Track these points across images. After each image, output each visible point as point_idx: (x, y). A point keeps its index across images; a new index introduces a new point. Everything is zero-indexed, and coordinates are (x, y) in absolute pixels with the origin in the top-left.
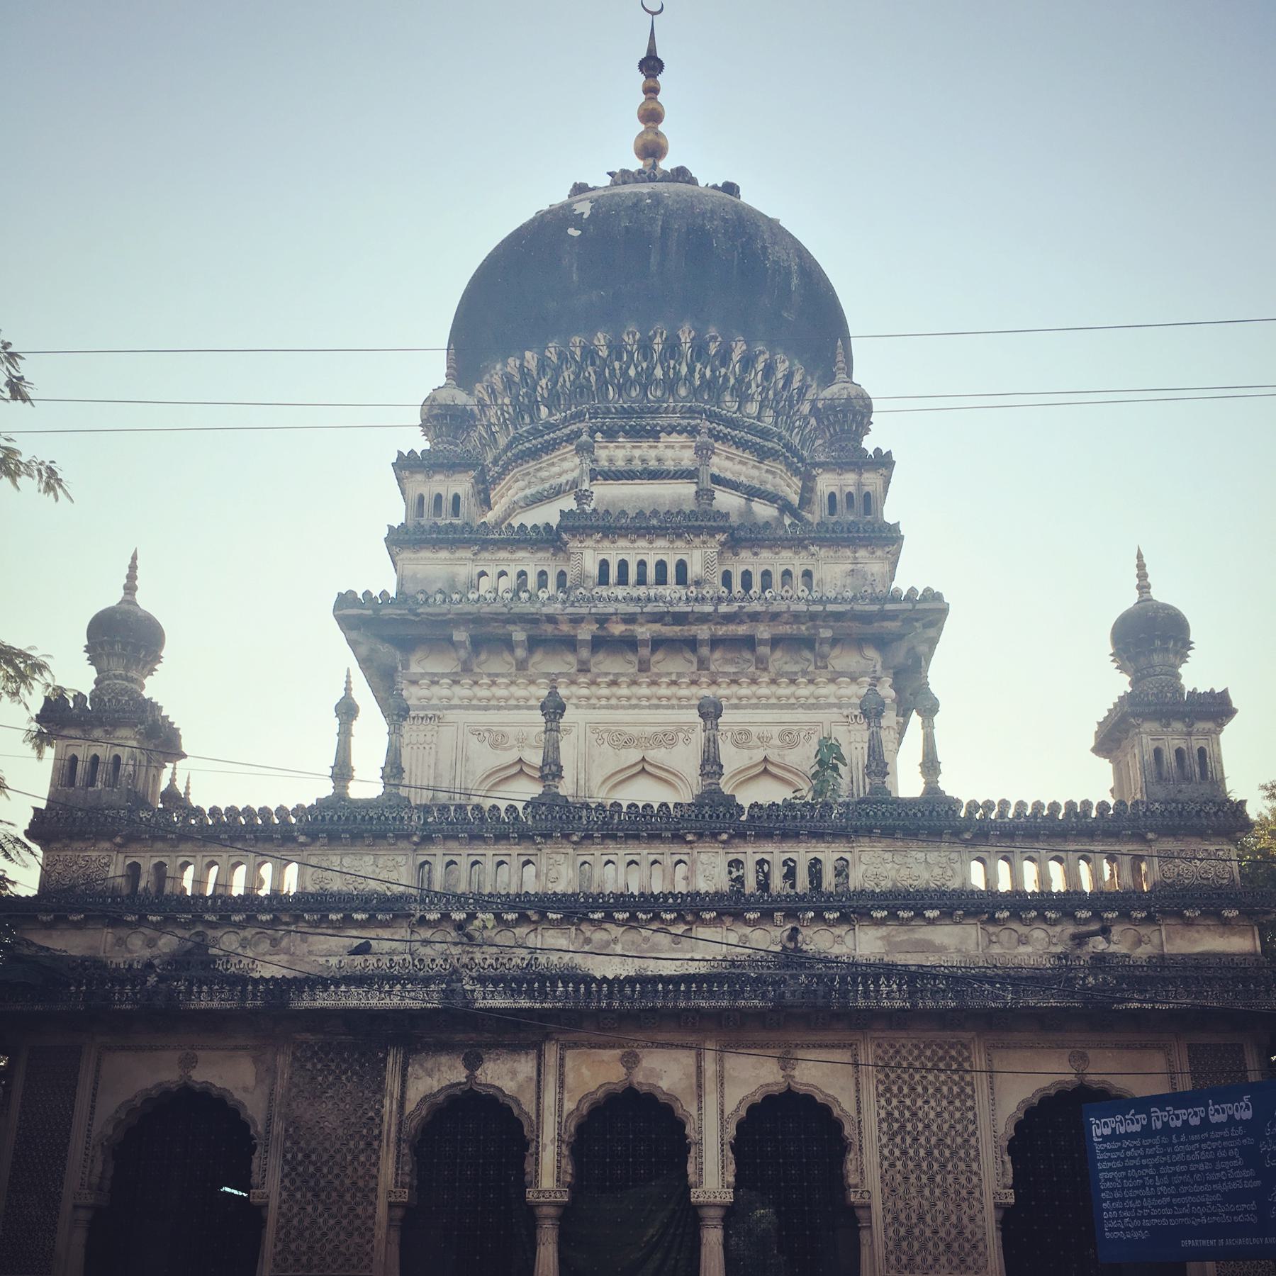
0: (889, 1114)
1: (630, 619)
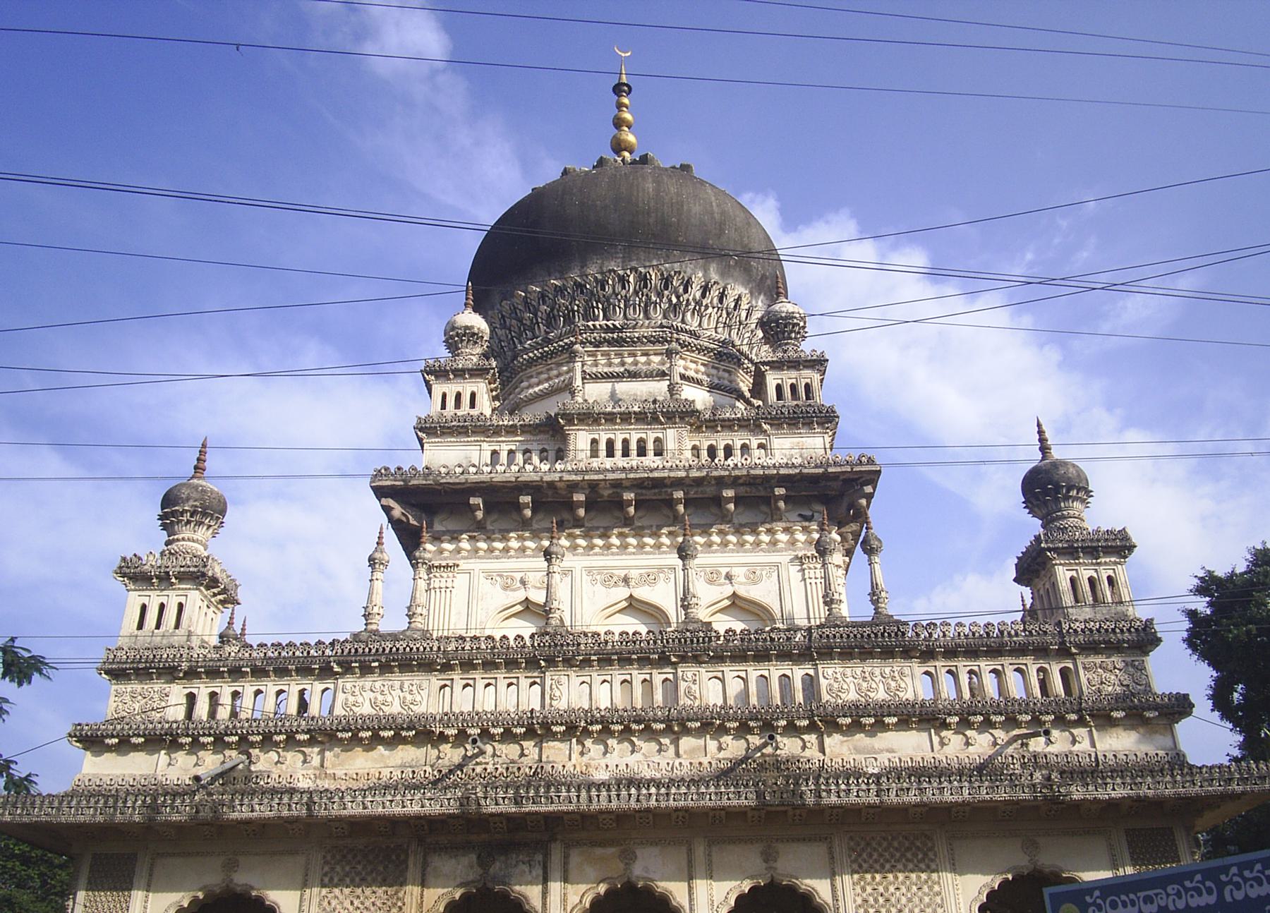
0: (865, 901)
1: (617, 484)
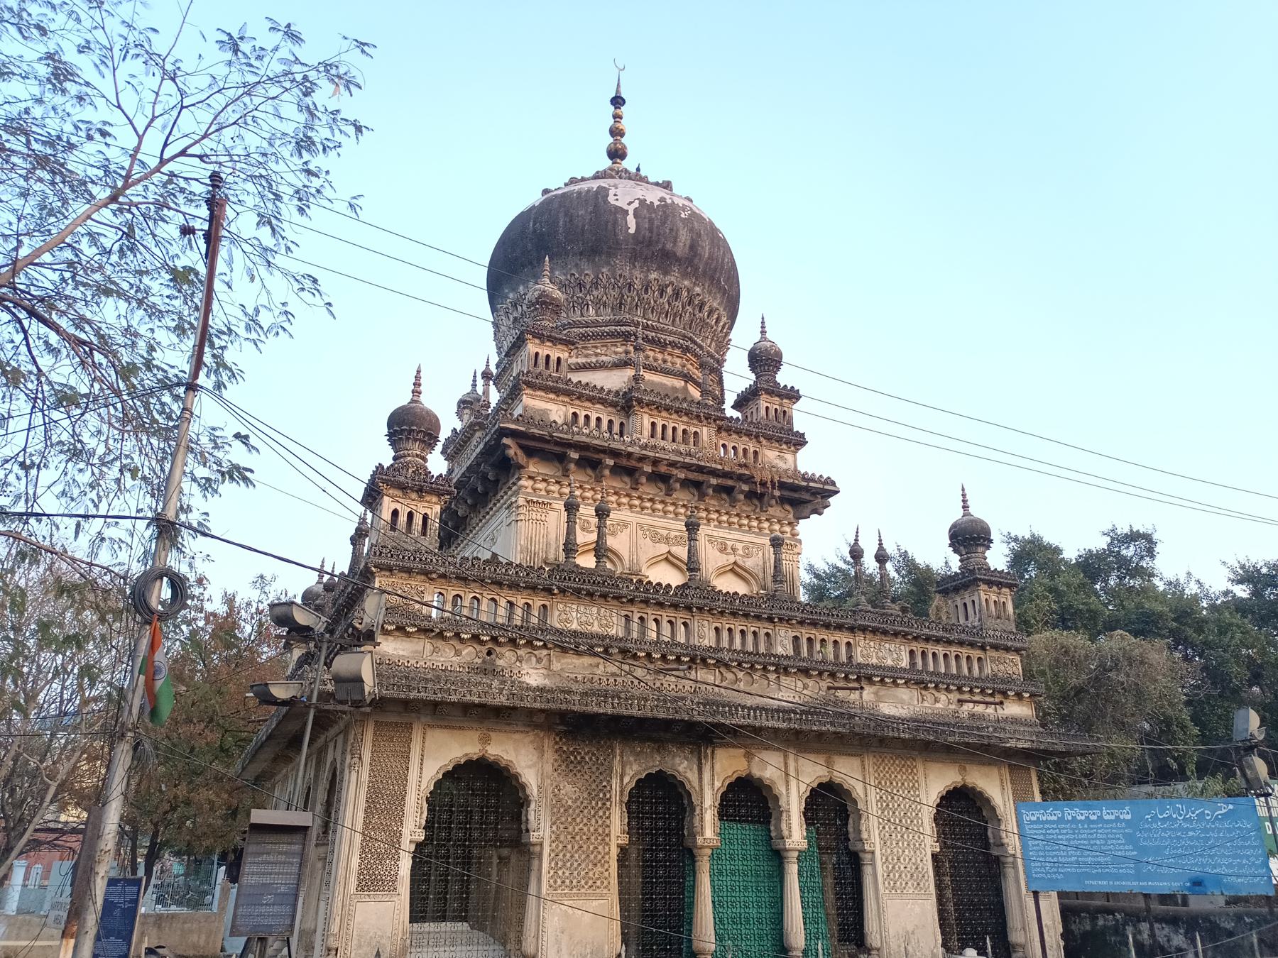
1: (673, 464)
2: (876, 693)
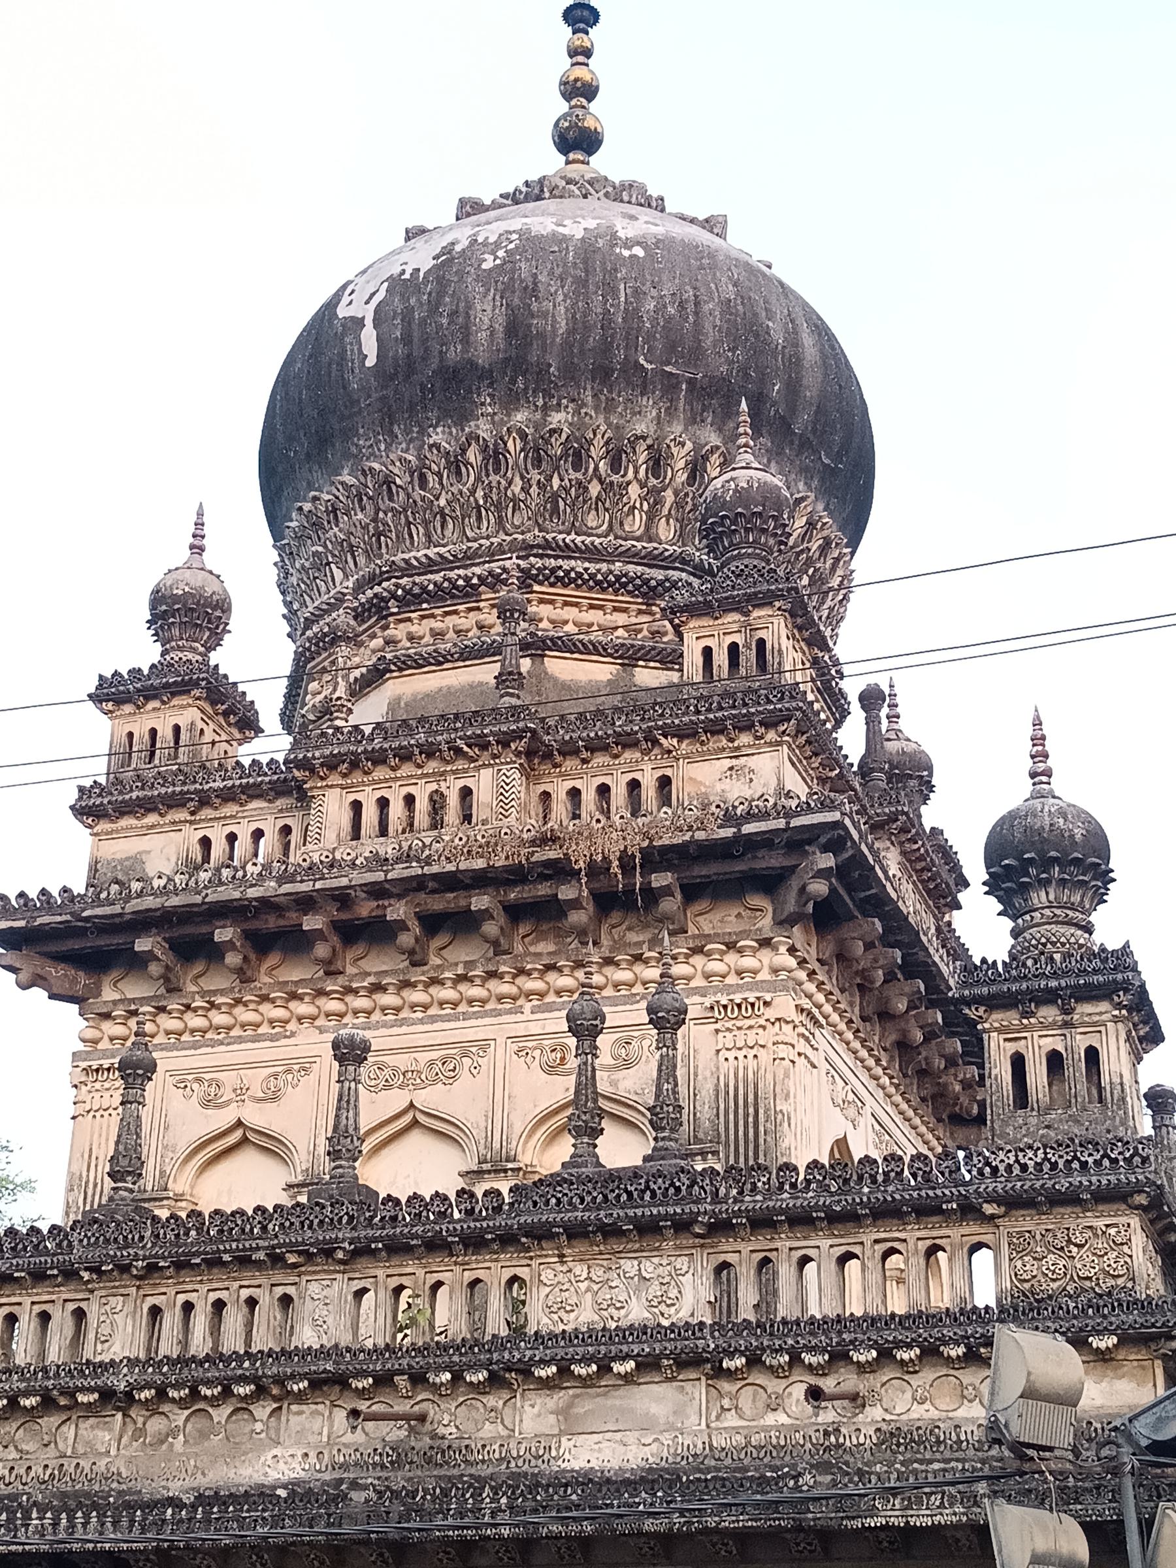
1: (377, 891)
2: (563, 1413)
